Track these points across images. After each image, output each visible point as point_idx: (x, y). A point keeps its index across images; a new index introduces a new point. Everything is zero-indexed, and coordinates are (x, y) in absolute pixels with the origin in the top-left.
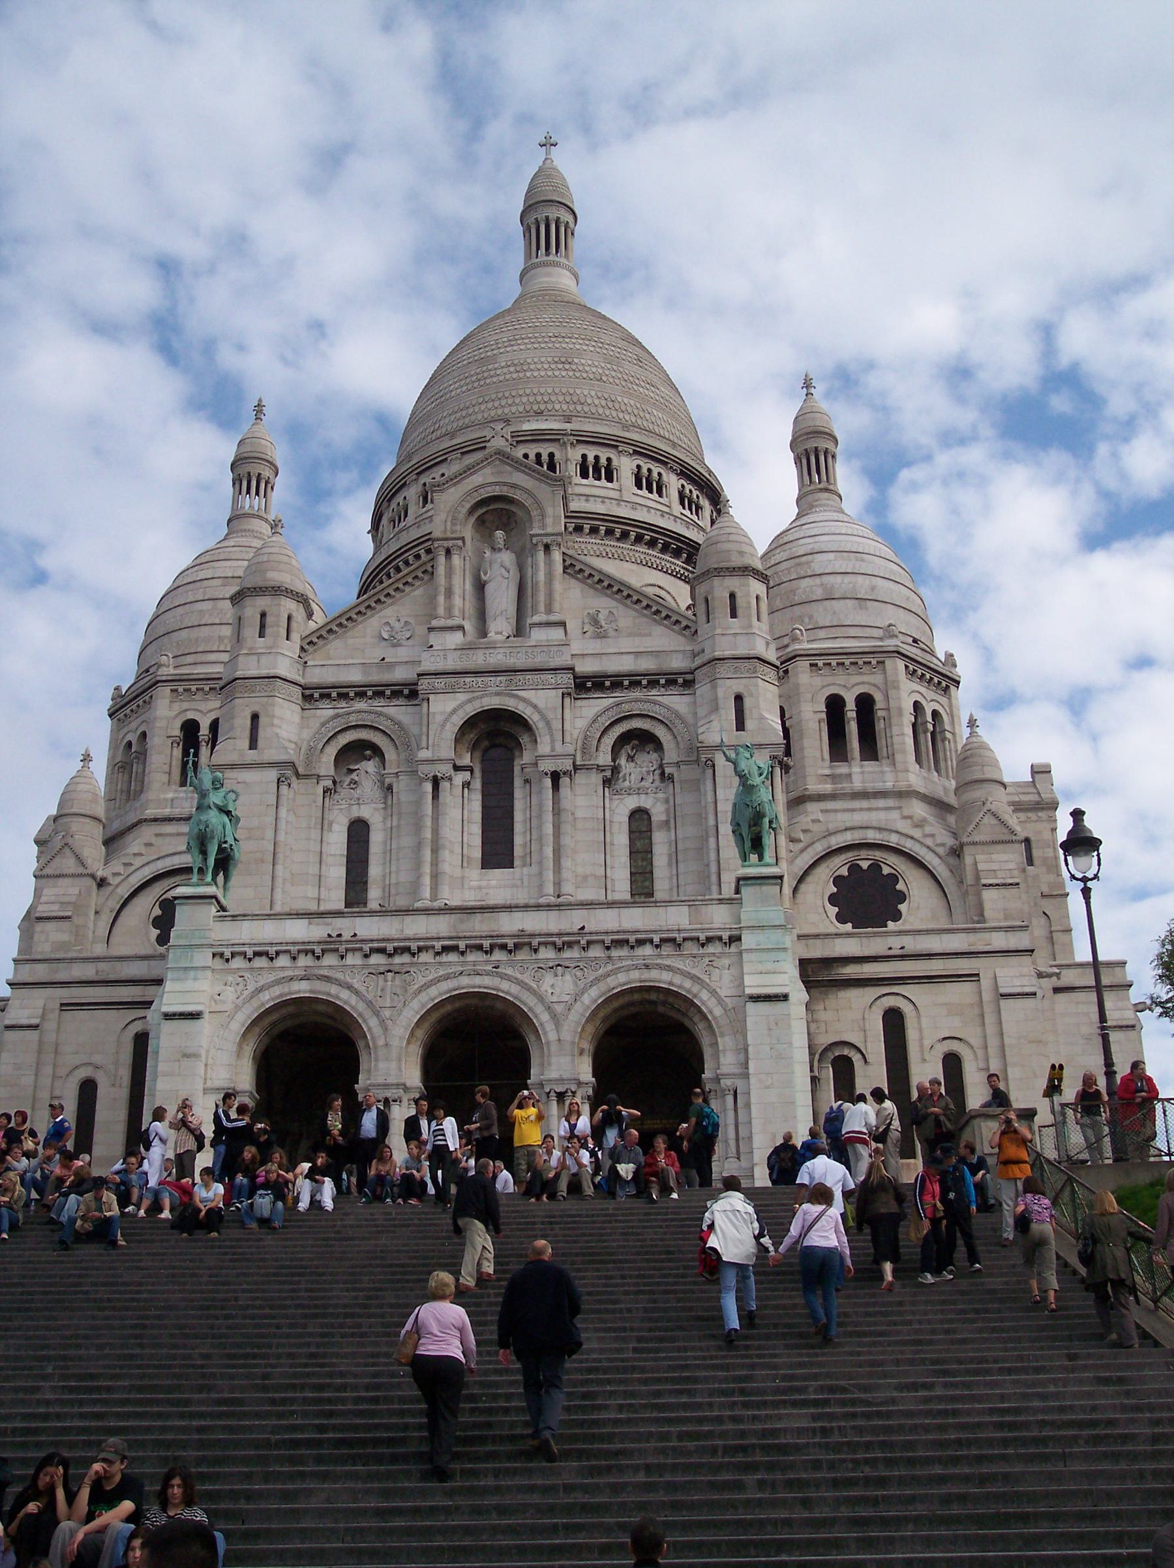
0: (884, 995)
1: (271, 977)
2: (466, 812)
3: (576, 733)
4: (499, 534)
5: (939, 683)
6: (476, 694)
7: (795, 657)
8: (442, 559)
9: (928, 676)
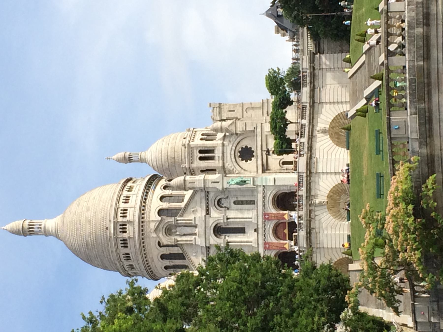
4: (173, 231)
7: (189, 168)
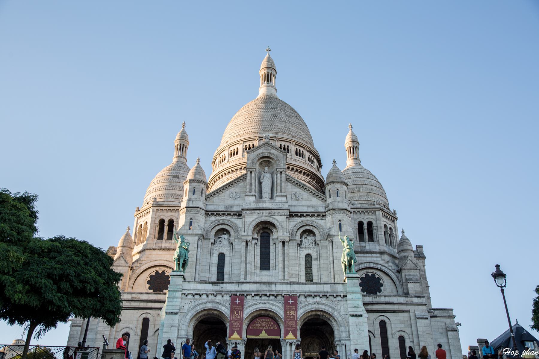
0: (380, 316)
1: (200, 302)
2: (255, 252)
3: (290, 229)
4: (266, 168)
5: (392, 219)
6: (260, 216)
8: (249, 175)
9: (388, 217)
